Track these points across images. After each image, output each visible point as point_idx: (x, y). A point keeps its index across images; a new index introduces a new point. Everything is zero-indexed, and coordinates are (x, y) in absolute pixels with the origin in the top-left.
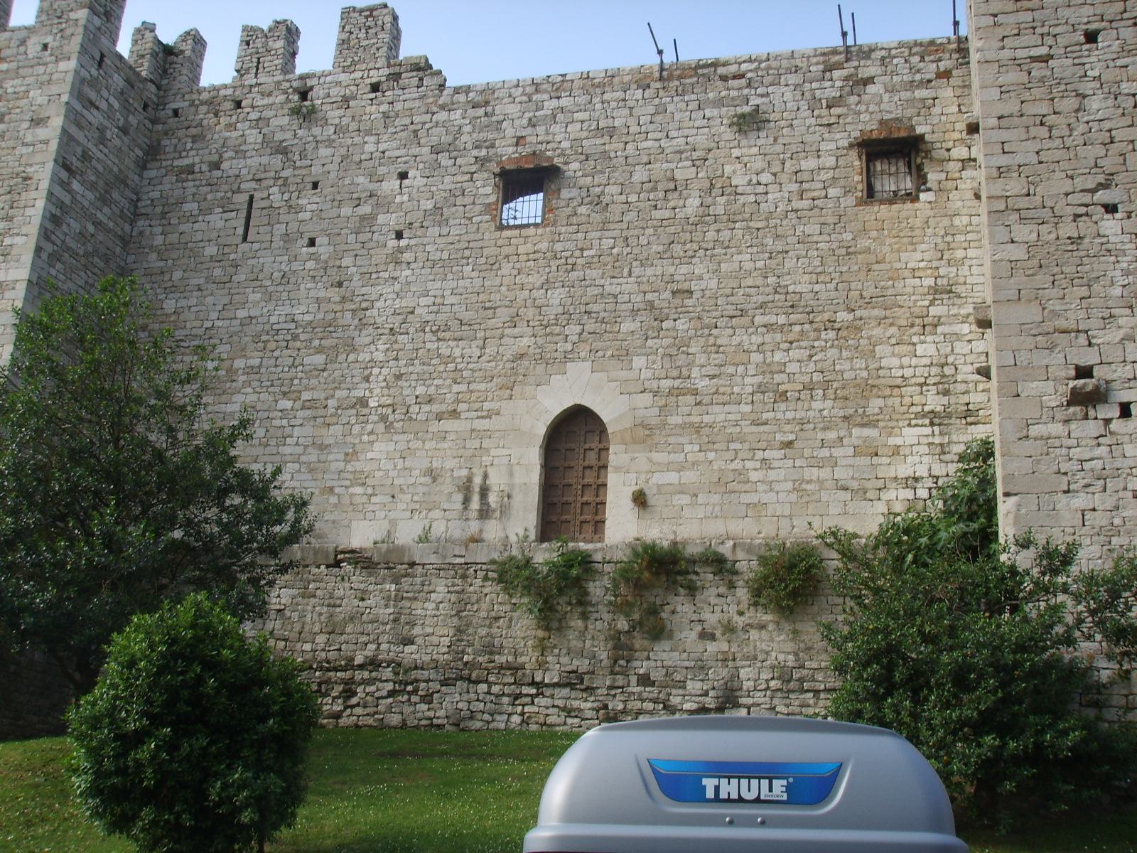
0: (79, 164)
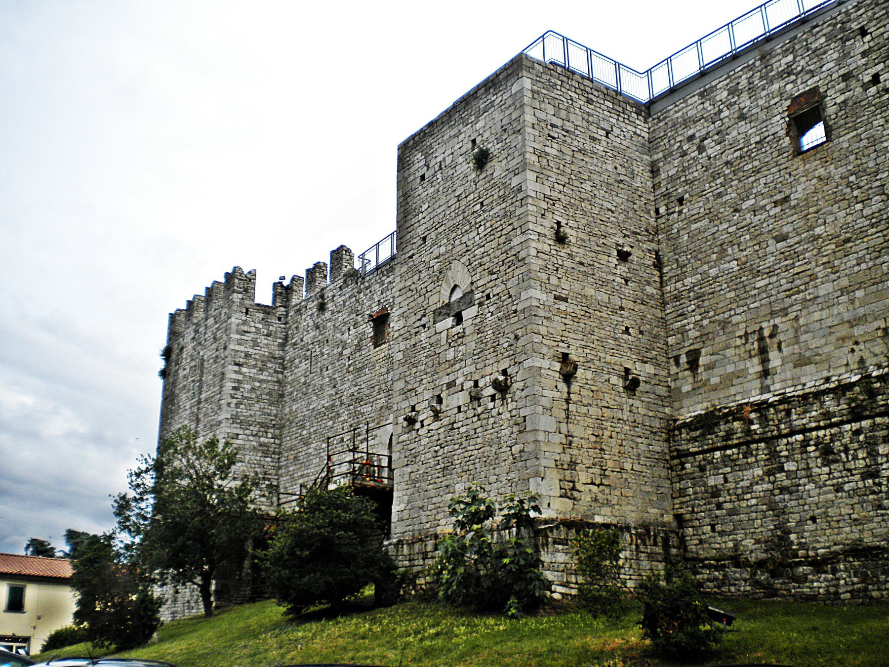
0: (244, 360)
